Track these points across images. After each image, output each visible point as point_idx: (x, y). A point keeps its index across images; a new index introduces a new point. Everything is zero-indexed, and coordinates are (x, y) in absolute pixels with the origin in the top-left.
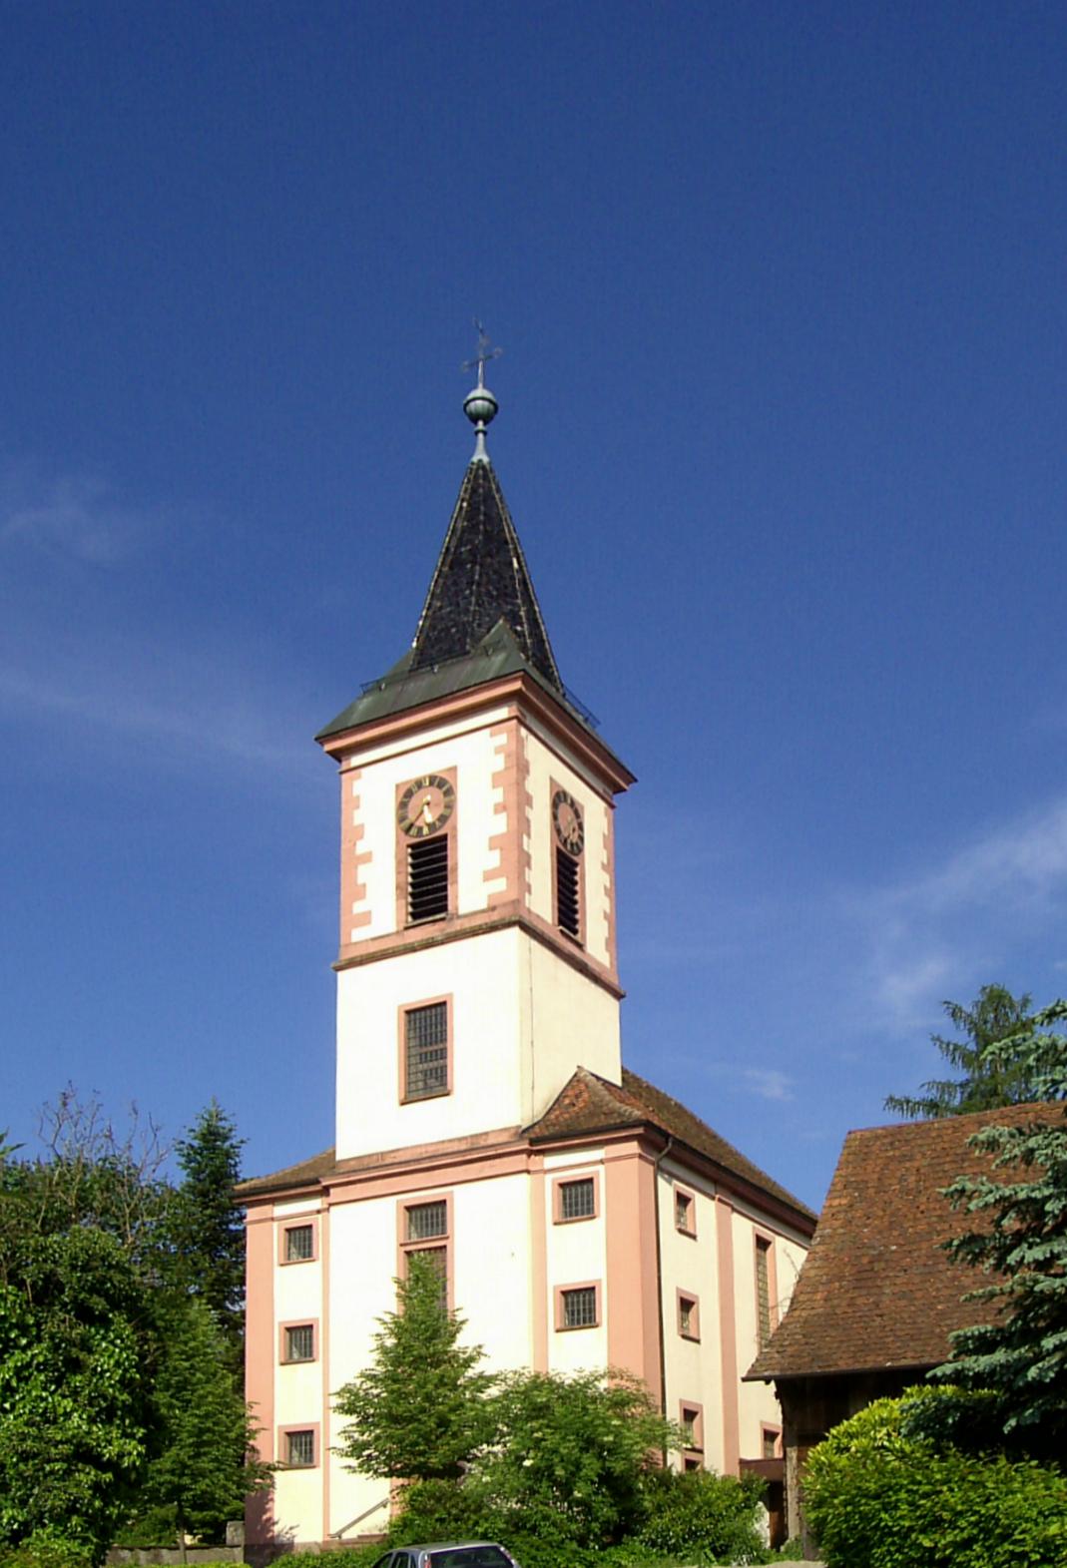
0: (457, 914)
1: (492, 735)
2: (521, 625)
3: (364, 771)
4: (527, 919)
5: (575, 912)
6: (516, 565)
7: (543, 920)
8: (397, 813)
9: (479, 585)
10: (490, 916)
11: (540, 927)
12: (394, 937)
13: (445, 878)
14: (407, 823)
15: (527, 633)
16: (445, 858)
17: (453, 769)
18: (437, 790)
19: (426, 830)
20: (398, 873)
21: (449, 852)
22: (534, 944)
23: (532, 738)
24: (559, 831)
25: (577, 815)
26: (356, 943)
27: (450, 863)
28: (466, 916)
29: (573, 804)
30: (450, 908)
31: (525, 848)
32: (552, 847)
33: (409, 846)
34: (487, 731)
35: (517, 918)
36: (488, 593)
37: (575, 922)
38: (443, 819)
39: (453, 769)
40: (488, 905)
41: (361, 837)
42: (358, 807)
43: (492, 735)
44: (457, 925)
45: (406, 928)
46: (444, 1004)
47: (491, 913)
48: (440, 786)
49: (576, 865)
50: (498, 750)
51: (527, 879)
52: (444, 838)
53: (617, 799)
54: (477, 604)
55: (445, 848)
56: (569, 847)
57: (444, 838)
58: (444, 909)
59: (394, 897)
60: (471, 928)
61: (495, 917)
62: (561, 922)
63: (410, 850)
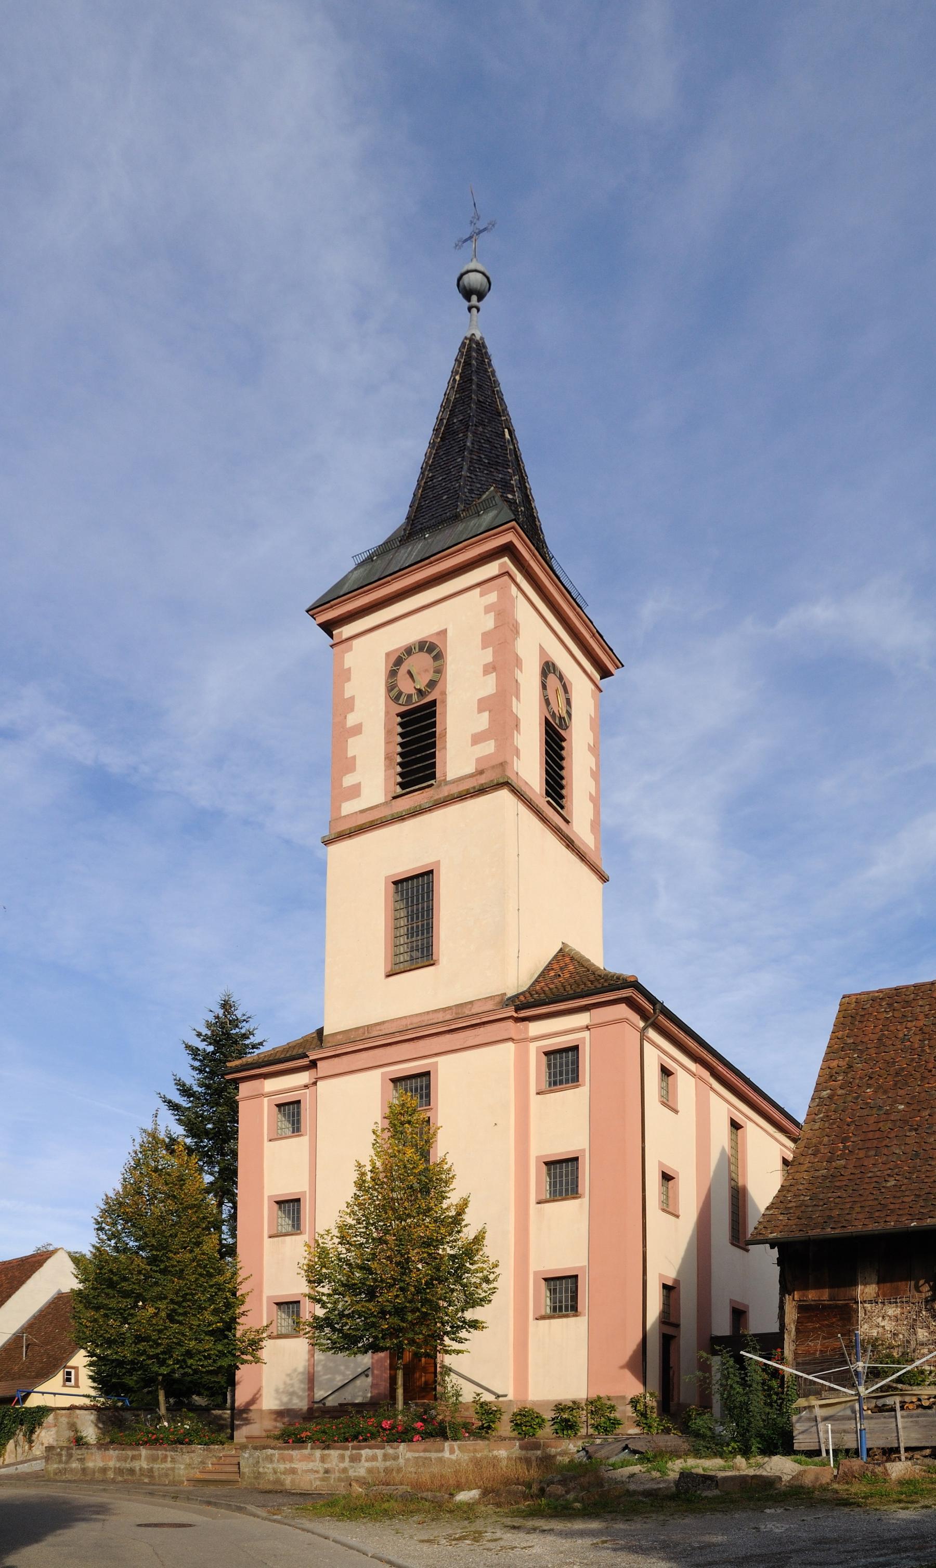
1: (482, 595)
3: (355, 642)
8: (387, 682)
9: (471, 452)
10: (477, 780)
13: (434, 745)
16: (434, 725)
17: (443, 633)
18: (426, 655)
21: (438, 718)
27: (438, 729)
28: (454, 781)
33: (398, 715)
34: (477, 591)
36: (480, 460)
38: (432, 684)
39: (443, 633)
41: (352, 710)
42: (349, 680)
43: (482, 595)
44: (445, 792)
45: (394, 798)
46: (431, 872)
47: (478, 777)
50: (488, 609)
52: (433, 703)
54: (469, 470)
55: (433, 714)
57: (433, 703)
58: (433, 776)
59: (383, 768)
61: (483, 780)
63: (399, 719)
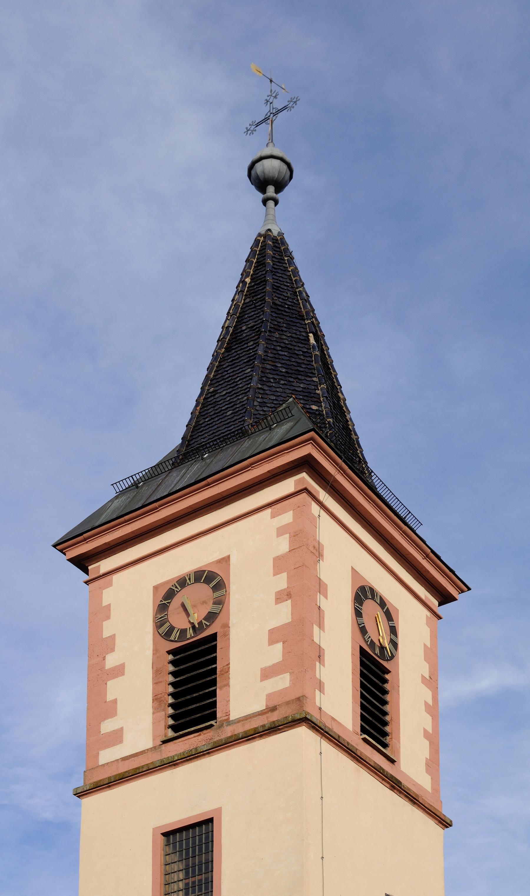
0: (228, 720)
1: (273, 516)
2: (318, 403)
3: (116, 577)
4: (315, 716)
5: (386, 724)
6: (312, 341)
7: (345, 728)
8: (155, 617)
9: (263, 361)
10: (267, 718)
11: (337, 730)
12: (150, 754)
13: (214, 683)
14: (165, 628)
15: (261, 241)
16: (214, 660)
17: (226, 560)
18: (205, 586)
19: (190, 633)
20: (156, 683)
21: (219, 654)
22: (327, 747)
23: (325, 516)
24: (363, 631)
25: (389, 616)
26: (103, 765)
27: (219, 665)
28: (239, 721)
29: (382, 604)
30: (219, 715)
31: (316, 640)
32: (353, 648)
33: (169, 652)
34: (269, 511)
35: (303, 715)
36: (275, 369)
37: (385, 734)
38: (211, 617)
39: (226, 560)
40: (267, 706)
41: (113, 650)
42: (108, 617)
43: (273, 516)
44: (228, 732)
45: (164, 742)
46: (211, 820)
47: (270, 714)
48: (215, 589)
49: (388, 672)
50: (281, 531)
51: (318, 676)
52: (214, 637)
53: (444, 610)
54: (260, 380)
55: (214, 649)
56: (377, 651)
57: (214, 637)
58: (213, 716)
59: (151, 711)
60: (245, 732)
61: (275, 717)
62: (363, 730)
63: (171, 657)
